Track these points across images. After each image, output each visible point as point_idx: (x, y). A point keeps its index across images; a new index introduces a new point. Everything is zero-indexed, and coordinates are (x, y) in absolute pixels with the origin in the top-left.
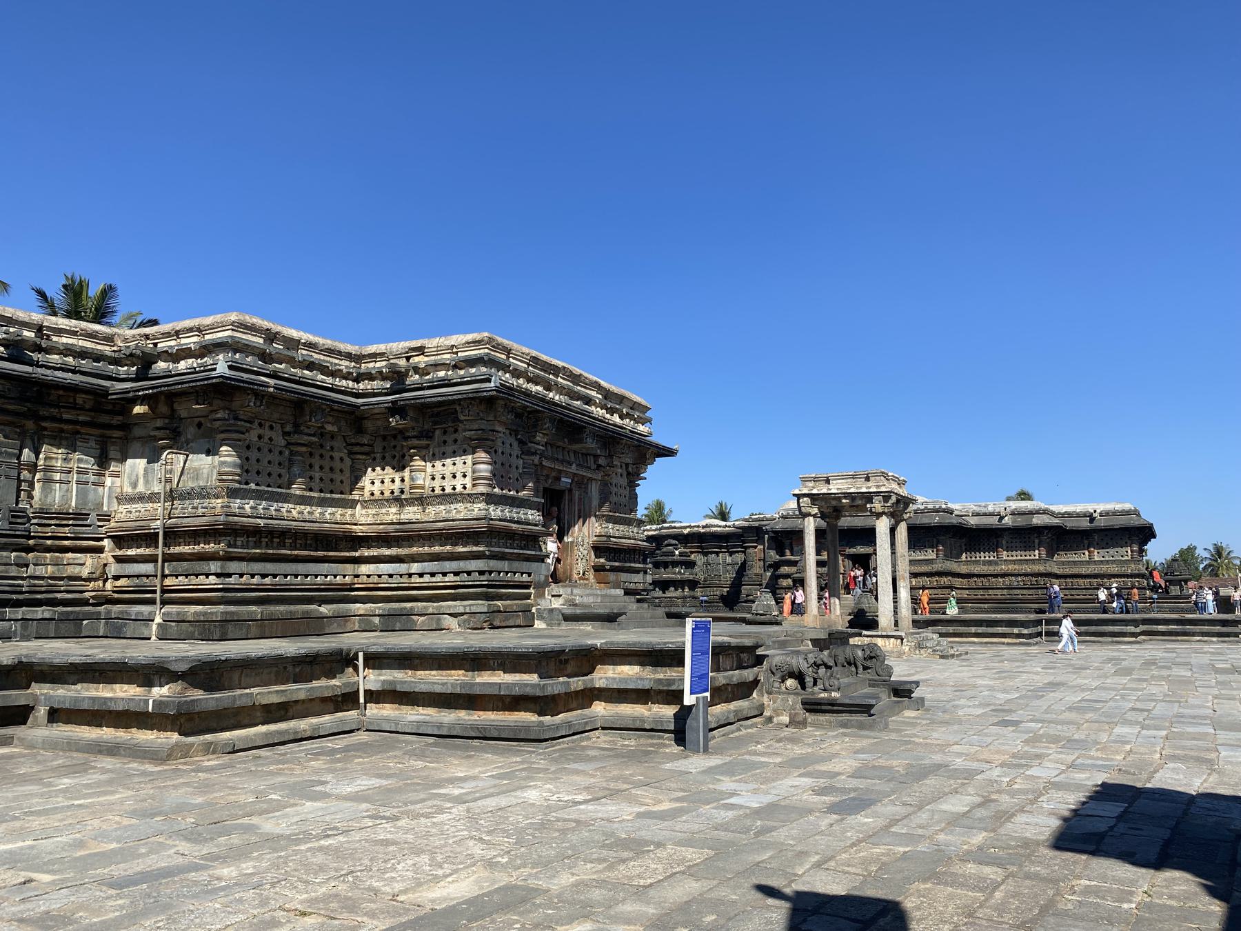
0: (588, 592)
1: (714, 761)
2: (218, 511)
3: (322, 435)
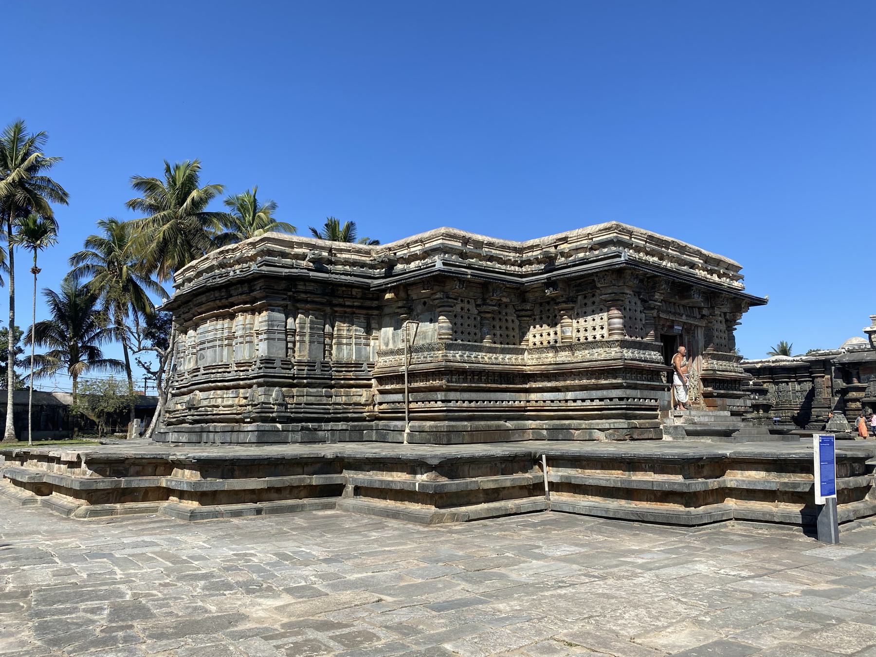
0: (702, 413)
1: (849, 552)
2: (440, 358)
3: (500, 305)
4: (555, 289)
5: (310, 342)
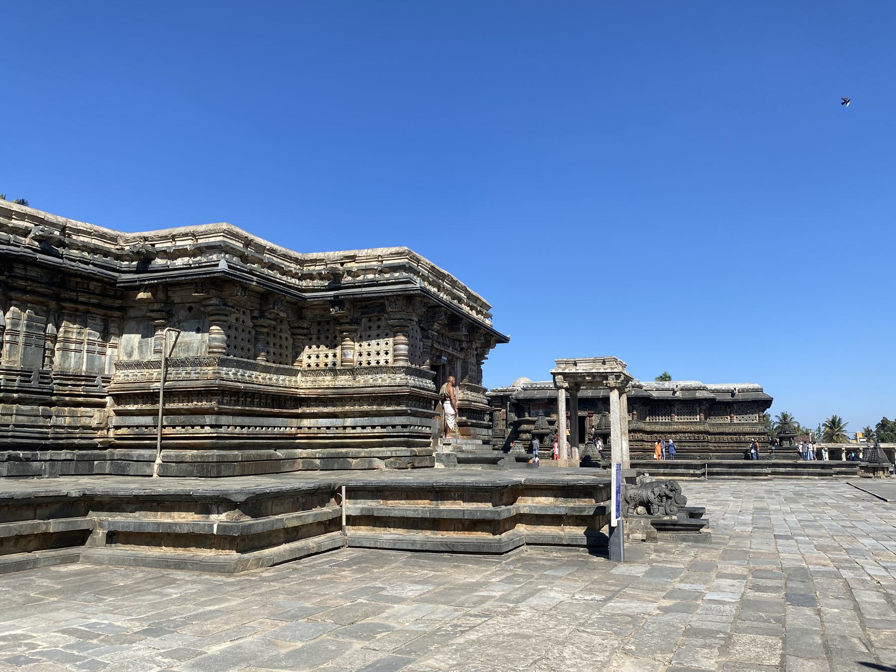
4: (341, 308)
5: (26, 344)
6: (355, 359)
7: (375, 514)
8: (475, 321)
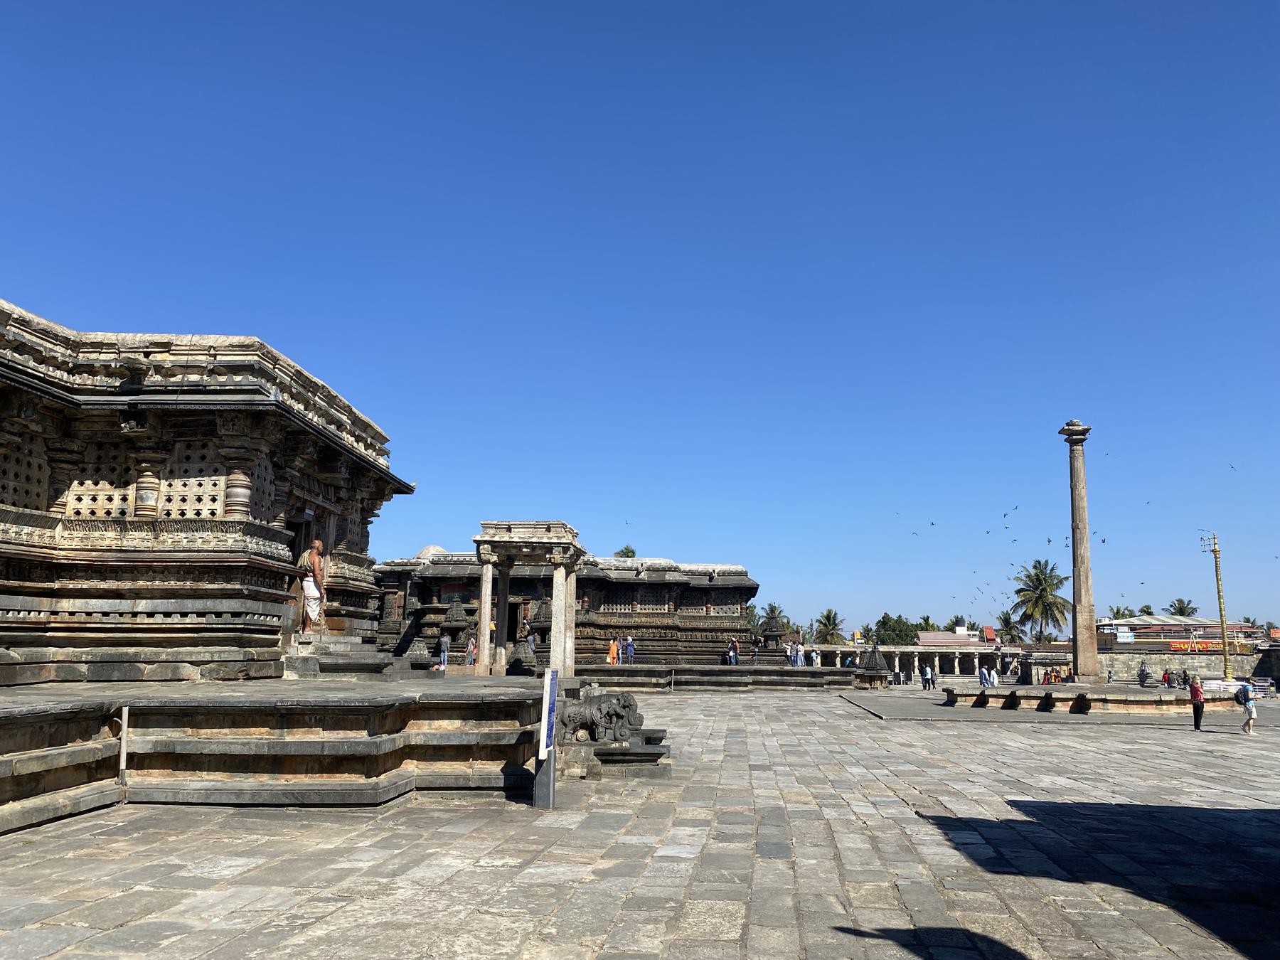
4: (140, 423)
6: (160, 507)
7: (178, 750)
8: (361, 458)
